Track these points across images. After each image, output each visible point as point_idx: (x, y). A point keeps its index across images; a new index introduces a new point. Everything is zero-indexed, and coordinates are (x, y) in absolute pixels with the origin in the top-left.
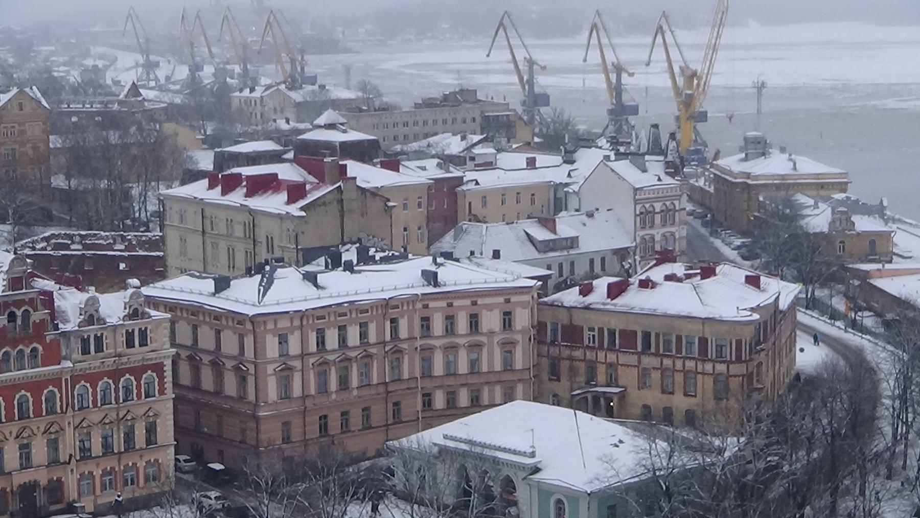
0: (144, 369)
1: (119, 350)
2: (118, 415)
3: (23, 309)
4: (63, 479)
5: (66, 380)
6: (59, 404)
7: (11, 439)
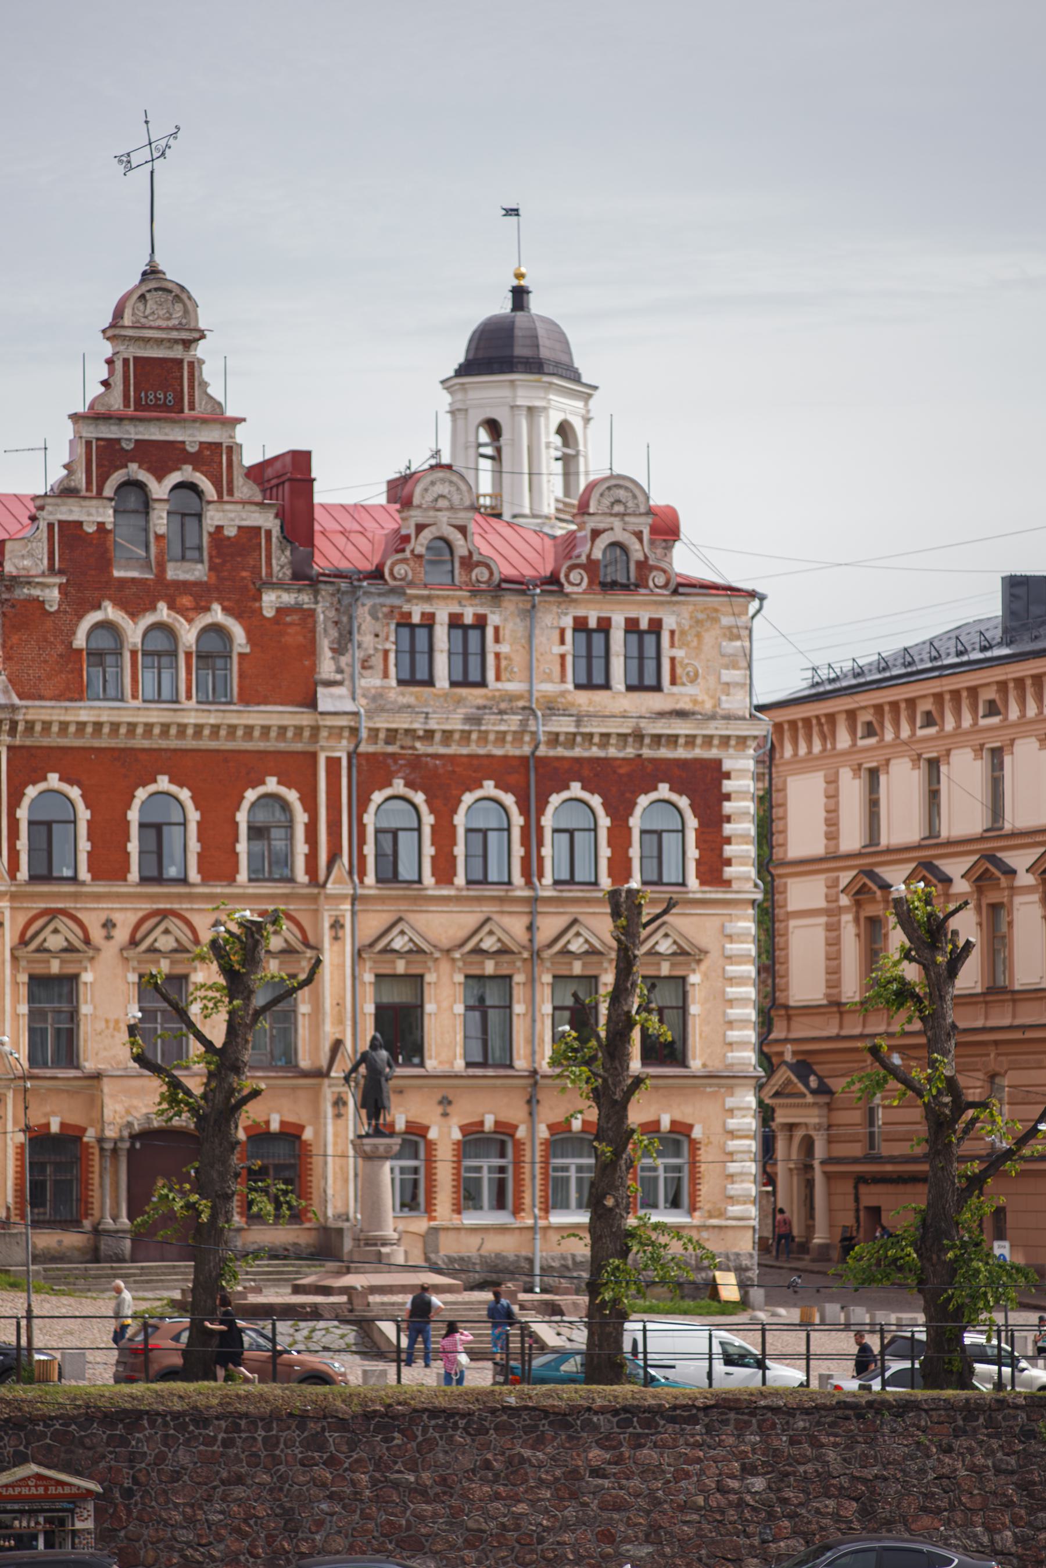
0: (644, 775)
1: (546, 688)
2: (530, 928)
3: (175, 478)
4: (308, 1135)
5: (333, 764)
6: (301, 848)
7: (110, 951)
